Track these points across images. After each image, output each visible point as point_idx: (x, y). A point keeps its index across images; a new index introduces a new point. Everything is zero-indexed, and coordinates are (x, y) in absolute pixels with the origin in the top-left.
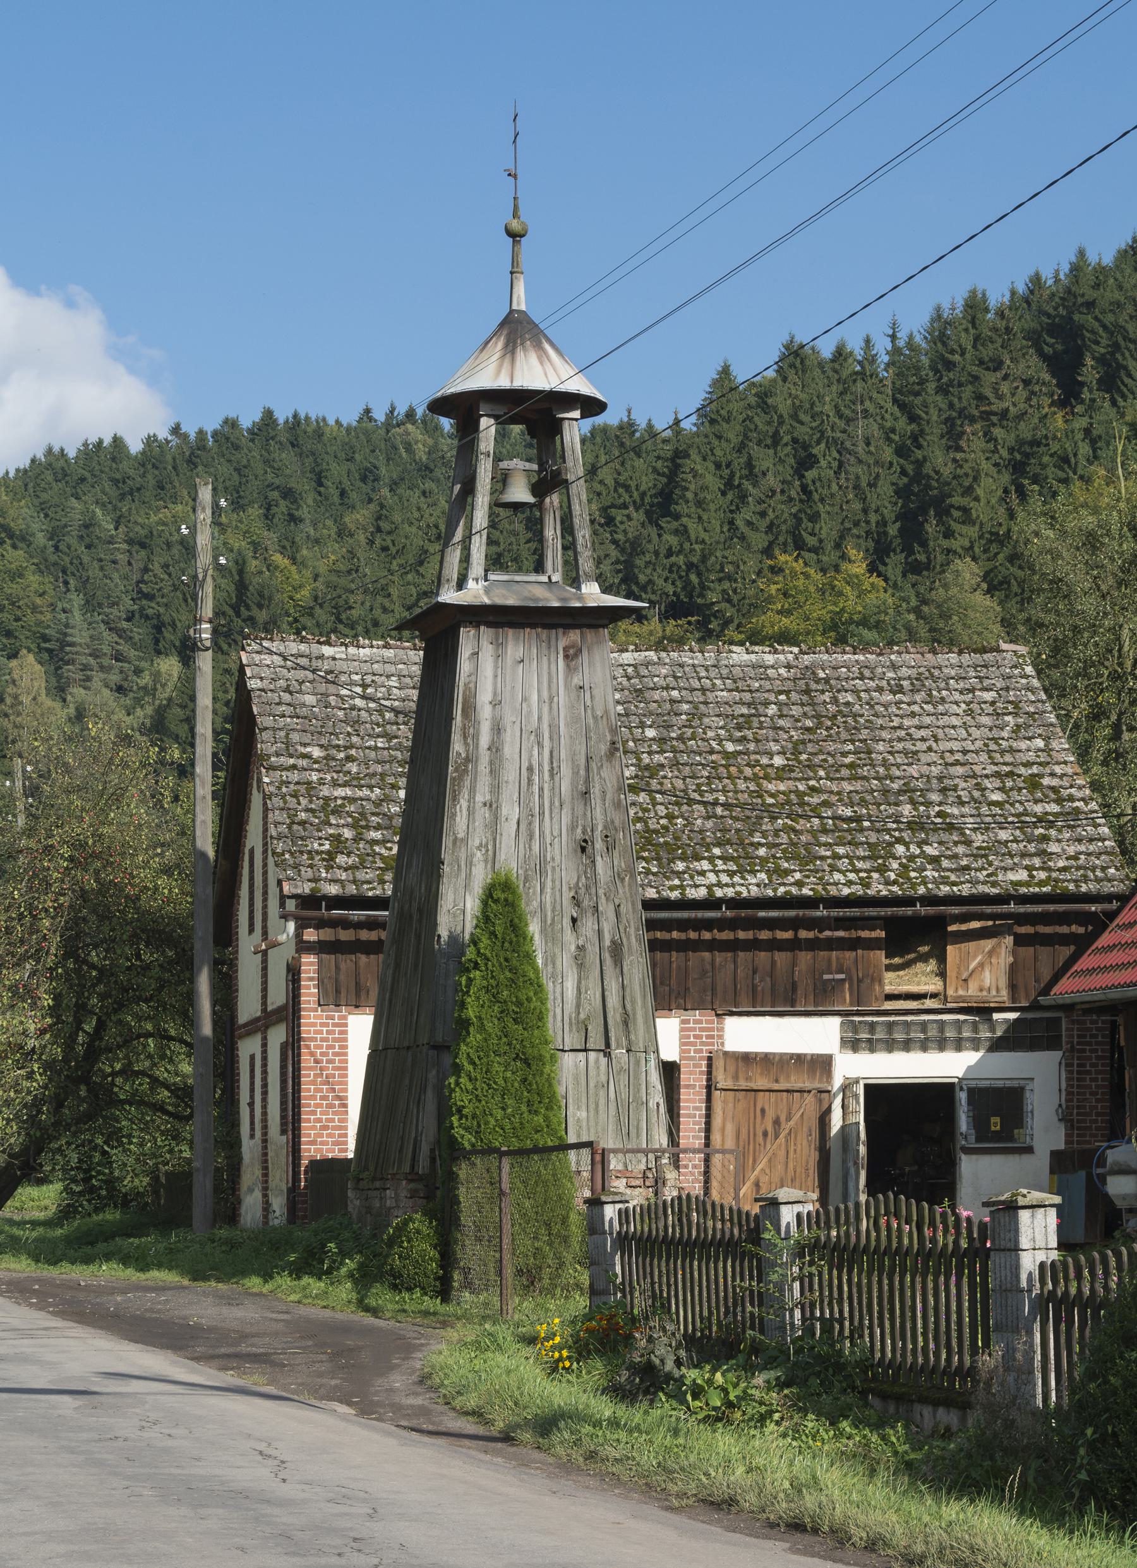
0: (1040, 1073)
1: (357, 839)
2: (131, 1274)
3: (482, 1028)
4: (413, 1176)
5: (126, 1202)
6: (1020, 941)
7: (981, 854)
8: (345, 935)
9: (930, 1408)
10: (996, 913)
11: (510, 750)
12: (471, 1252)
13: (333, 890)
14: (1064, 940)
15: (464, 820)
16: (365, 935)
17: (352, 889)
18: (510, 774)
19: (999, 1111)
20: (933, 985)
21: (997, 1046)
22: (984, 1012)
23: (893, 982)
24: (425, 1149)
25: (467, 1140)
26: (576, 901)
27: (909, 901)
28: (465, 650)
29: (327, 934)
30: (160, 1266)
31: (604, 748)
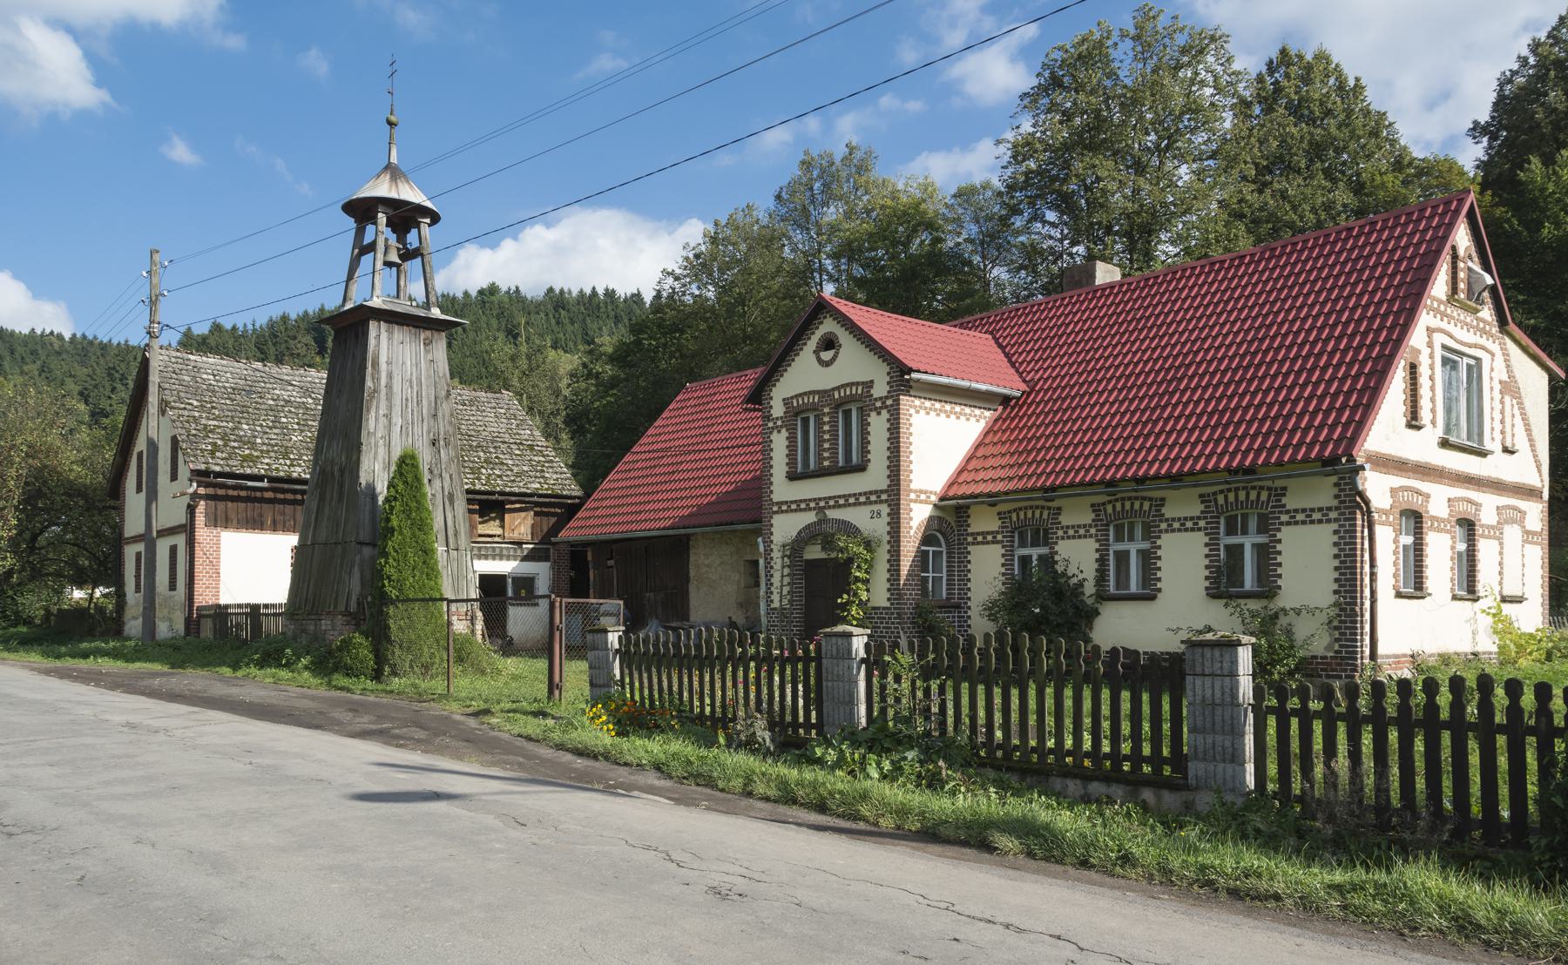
0: (541, 572)
1: (225, 445)
2: (120, 664)
3: (401, 533)
4: (347, 613)
5: (28, 622)
6: (536, 514)
7: (518, 475)
8: (221, 492)
9: (1078, 782)
10: (527, 501)
11: (397, 388)
12: (396, 654)
13: (217, 469)
14: (553, 514)
15: (373, 422)
16: (231, 492)
17: (227, 469)
18: (397, 401)
19: (525, 585)
20: (499, 531)
21: (525, 559)
22: (520, 544)
23: (482, 529)
24: (354, 598)
25: (394, 593)
26: (431, 471)
27: (492, 493)
28: (373, 333)
29: (210, 491)
30: (139, 660)
31: (444, 393)
